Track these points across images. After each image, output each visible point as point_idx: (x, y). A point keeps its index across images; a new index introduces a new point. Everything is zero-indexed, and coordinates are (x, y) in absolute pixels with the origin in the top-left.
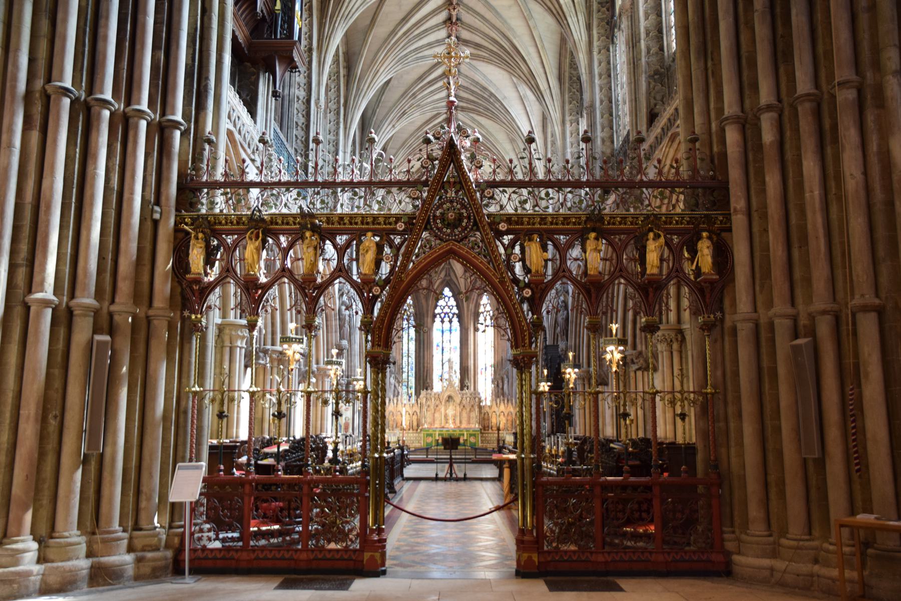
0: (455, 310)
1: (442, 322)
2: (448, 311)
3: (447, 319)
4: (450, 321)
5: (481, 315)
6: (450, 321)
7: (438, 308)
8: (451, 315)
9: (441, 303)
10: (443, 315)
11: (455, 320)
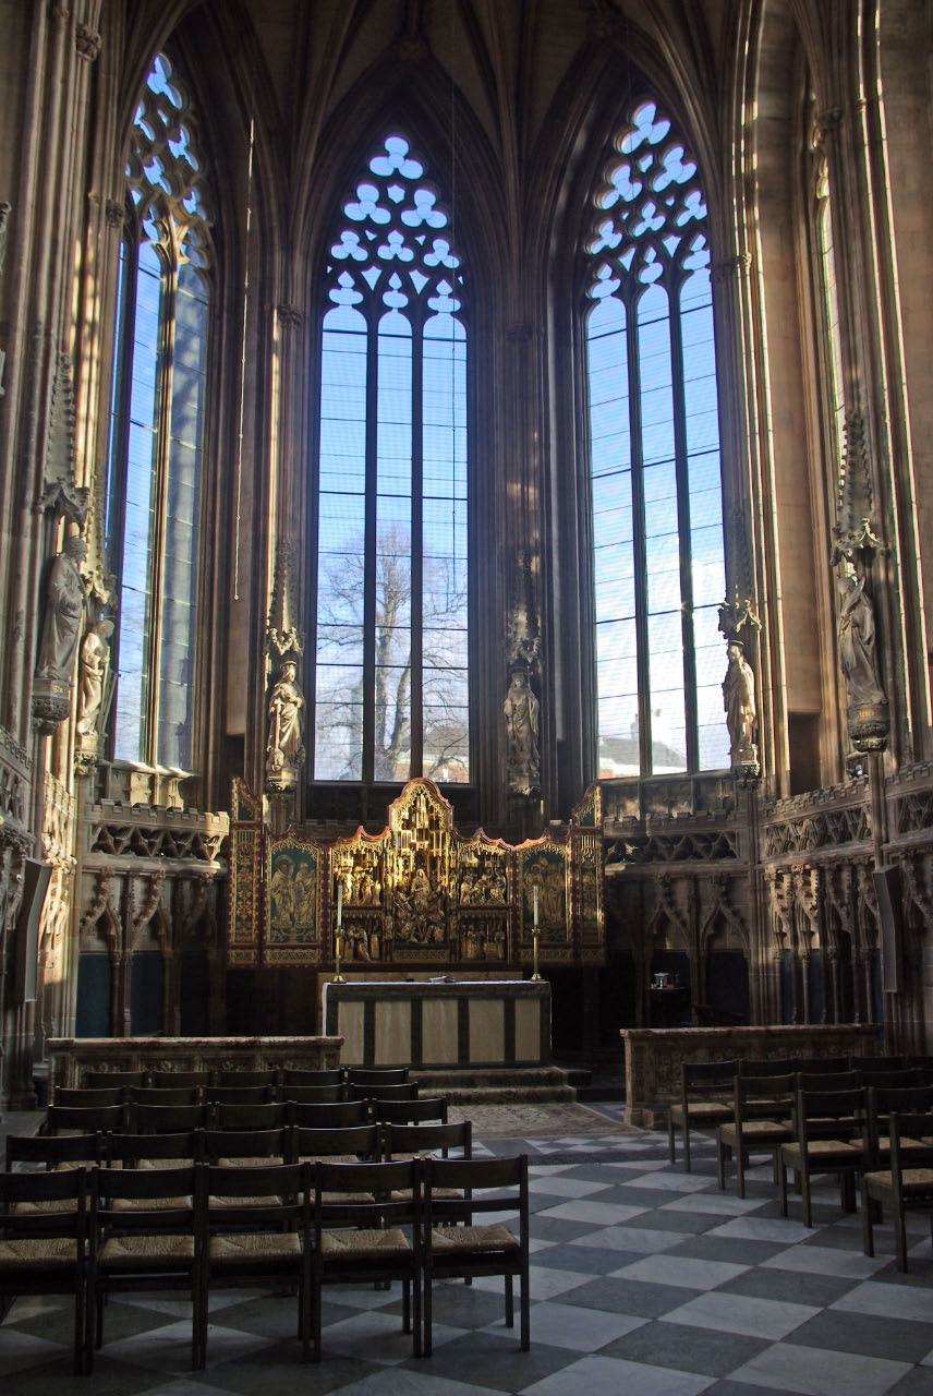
0: (441, 254)
1: (372, 307)
2: (407, 255)
3: (395, 299)
4: (418, 312)
5: (606, 271)
6: (418, 312)
7: (349, 239)
8: (419, 281)
9: (365, 205)
10: (372, 276)
11: (444, 302)
